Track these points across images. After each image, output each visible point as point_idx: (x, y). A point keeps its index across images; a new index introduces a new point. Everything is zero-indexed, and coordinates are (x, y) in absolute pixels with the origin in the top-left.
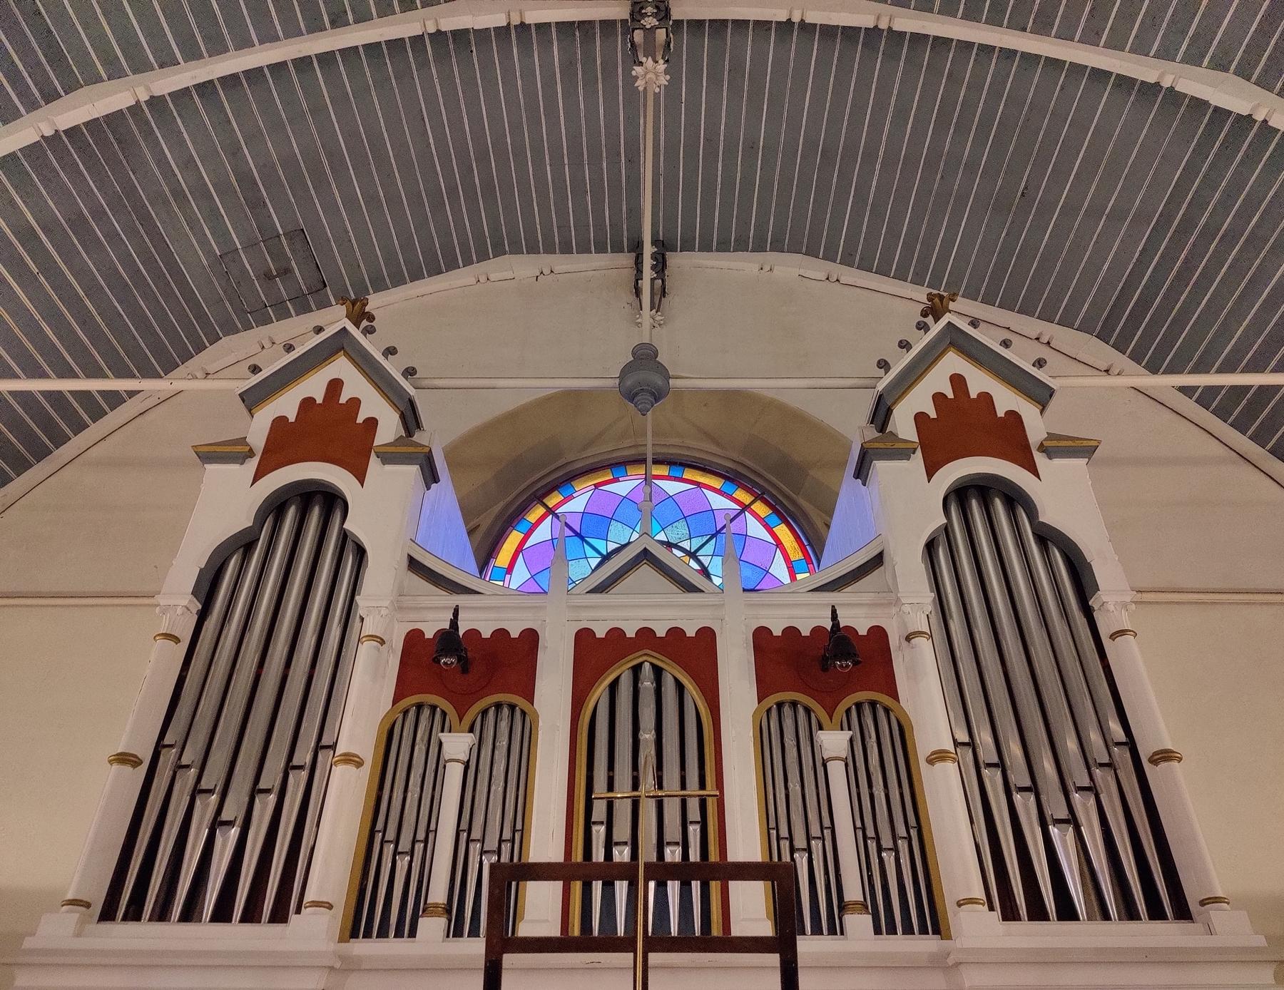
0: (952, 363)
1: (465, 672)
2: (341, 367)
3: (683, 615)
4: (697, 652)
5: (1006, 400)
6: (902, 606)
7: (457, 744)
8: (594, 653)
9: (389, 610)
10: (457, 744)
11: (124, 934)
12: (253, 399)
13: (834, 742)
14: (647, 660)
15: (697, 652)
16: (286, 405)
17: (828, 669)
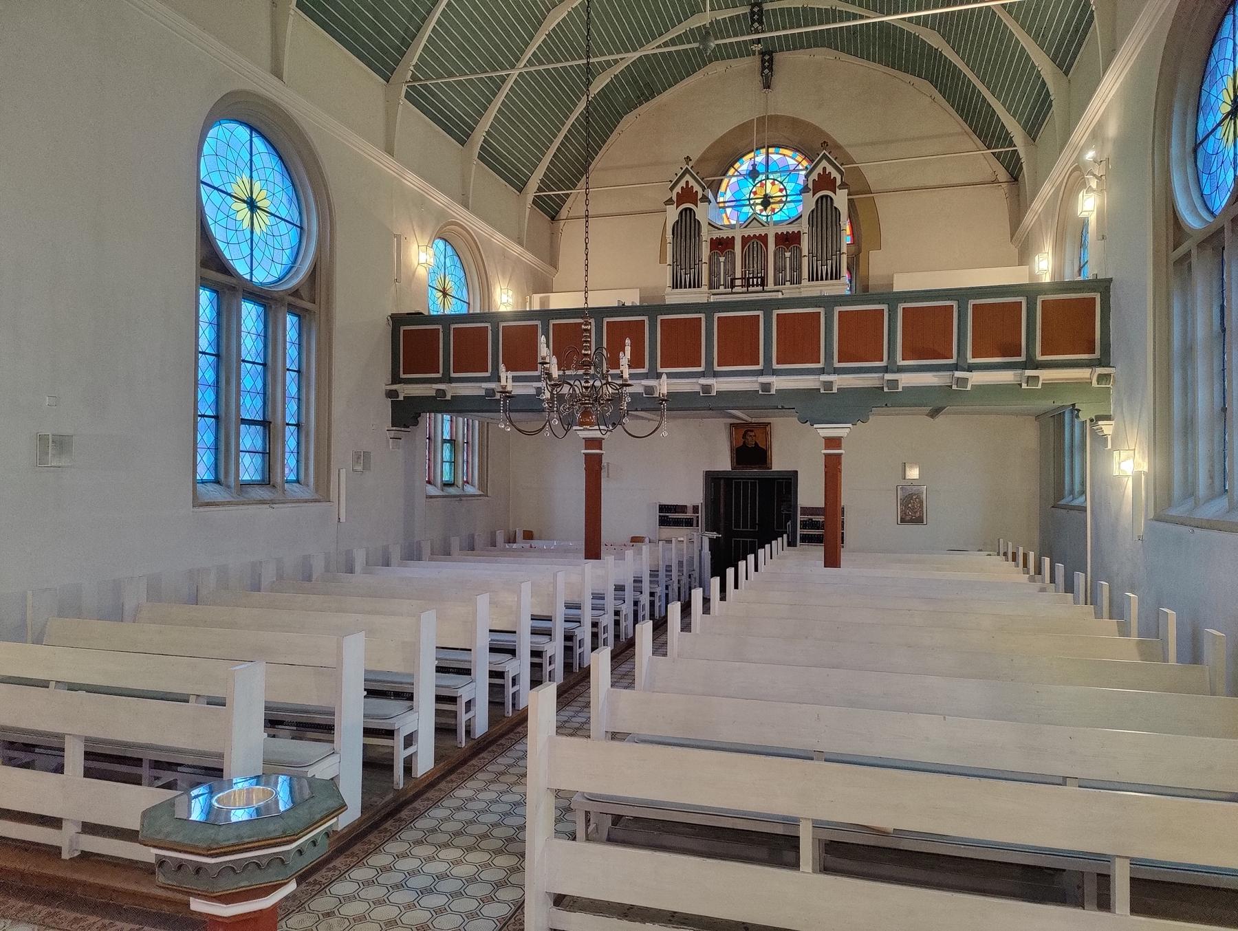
0: (824, 163)
1: (722, 245)
2: (688, 177)
3: (762, 231)
4: (764, 239)
5: (835, 174)
6: (804, 227)
7: (722, 259)
8: (745, 240)
9: (706, 234)
10: (722, 259)
11: (676, 291)
12: (672, 189)
13: (788, 254)
14: (755, 241)
15: (764, 239)
16: (678, 189)
17: (788, 240)
